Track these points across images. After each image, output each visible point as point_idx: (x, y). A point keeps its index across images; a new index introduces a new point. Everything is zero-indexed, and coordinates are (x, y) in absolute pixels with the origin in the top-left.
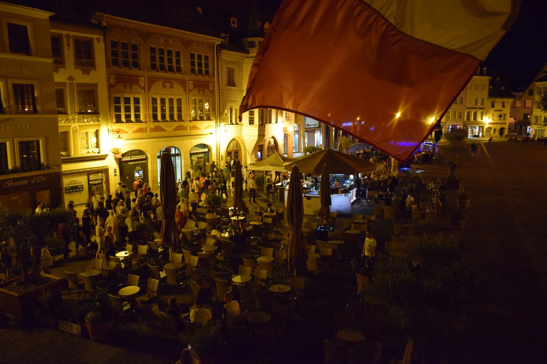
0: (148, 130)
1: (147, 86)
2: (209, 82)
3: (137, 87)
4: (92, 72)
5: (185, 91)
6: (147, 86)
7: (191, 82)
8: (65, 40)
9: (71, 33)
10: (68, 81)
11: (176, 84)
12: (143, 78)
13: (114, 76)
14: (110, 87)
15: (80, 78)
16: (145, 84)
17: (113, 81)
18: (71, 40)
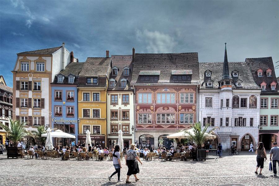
0: (154, 127)
1: (154, 109)
2: (192, 106)
3: (149, 110)
4: (128, 105)
5: (176, 111)
6: (154, 109)
7: (180, 106)
8: (119, 96)
9: (121, 93)
10: (119, 109)
11: (170, 108)
12: (152, 106)
13: (139, 106)
14: (136, 110)
15: (124, 108)
16: (153, 109)
17: (138, 108)
18: (121, 96)
